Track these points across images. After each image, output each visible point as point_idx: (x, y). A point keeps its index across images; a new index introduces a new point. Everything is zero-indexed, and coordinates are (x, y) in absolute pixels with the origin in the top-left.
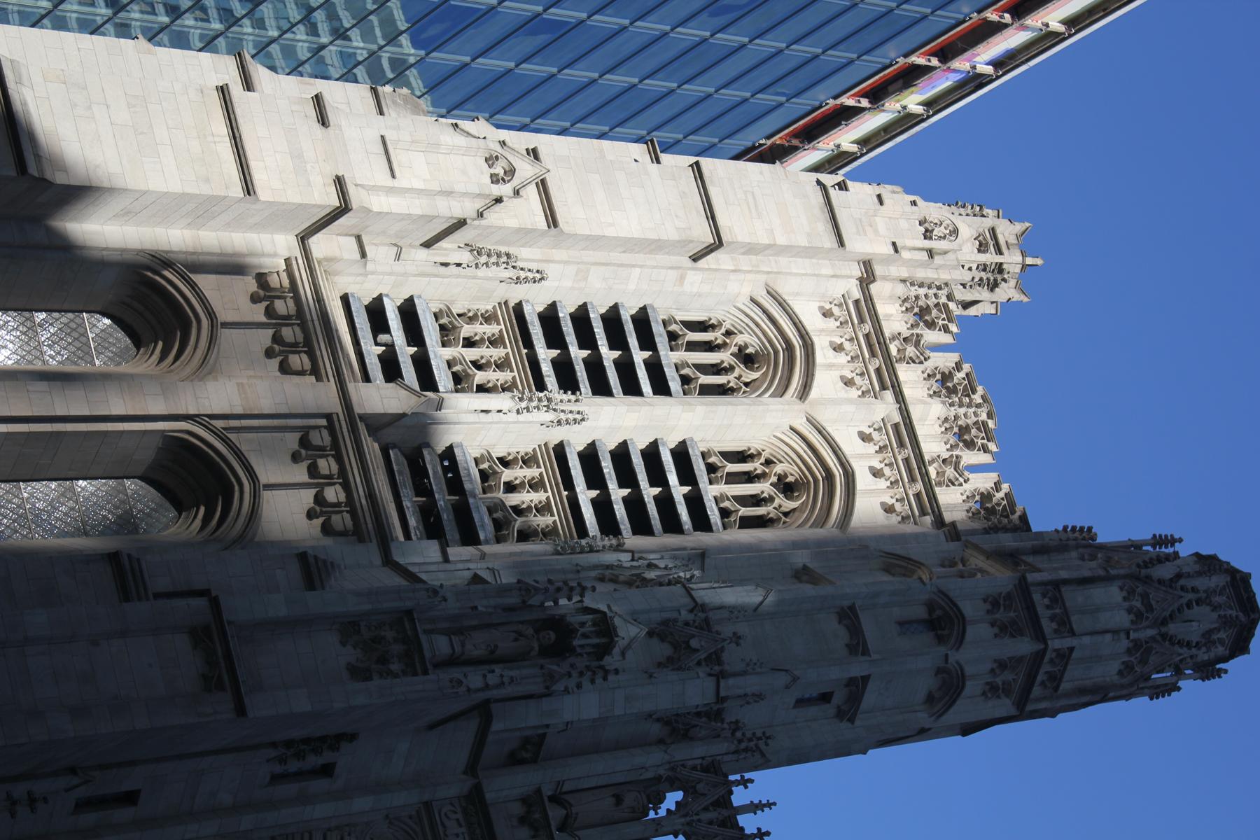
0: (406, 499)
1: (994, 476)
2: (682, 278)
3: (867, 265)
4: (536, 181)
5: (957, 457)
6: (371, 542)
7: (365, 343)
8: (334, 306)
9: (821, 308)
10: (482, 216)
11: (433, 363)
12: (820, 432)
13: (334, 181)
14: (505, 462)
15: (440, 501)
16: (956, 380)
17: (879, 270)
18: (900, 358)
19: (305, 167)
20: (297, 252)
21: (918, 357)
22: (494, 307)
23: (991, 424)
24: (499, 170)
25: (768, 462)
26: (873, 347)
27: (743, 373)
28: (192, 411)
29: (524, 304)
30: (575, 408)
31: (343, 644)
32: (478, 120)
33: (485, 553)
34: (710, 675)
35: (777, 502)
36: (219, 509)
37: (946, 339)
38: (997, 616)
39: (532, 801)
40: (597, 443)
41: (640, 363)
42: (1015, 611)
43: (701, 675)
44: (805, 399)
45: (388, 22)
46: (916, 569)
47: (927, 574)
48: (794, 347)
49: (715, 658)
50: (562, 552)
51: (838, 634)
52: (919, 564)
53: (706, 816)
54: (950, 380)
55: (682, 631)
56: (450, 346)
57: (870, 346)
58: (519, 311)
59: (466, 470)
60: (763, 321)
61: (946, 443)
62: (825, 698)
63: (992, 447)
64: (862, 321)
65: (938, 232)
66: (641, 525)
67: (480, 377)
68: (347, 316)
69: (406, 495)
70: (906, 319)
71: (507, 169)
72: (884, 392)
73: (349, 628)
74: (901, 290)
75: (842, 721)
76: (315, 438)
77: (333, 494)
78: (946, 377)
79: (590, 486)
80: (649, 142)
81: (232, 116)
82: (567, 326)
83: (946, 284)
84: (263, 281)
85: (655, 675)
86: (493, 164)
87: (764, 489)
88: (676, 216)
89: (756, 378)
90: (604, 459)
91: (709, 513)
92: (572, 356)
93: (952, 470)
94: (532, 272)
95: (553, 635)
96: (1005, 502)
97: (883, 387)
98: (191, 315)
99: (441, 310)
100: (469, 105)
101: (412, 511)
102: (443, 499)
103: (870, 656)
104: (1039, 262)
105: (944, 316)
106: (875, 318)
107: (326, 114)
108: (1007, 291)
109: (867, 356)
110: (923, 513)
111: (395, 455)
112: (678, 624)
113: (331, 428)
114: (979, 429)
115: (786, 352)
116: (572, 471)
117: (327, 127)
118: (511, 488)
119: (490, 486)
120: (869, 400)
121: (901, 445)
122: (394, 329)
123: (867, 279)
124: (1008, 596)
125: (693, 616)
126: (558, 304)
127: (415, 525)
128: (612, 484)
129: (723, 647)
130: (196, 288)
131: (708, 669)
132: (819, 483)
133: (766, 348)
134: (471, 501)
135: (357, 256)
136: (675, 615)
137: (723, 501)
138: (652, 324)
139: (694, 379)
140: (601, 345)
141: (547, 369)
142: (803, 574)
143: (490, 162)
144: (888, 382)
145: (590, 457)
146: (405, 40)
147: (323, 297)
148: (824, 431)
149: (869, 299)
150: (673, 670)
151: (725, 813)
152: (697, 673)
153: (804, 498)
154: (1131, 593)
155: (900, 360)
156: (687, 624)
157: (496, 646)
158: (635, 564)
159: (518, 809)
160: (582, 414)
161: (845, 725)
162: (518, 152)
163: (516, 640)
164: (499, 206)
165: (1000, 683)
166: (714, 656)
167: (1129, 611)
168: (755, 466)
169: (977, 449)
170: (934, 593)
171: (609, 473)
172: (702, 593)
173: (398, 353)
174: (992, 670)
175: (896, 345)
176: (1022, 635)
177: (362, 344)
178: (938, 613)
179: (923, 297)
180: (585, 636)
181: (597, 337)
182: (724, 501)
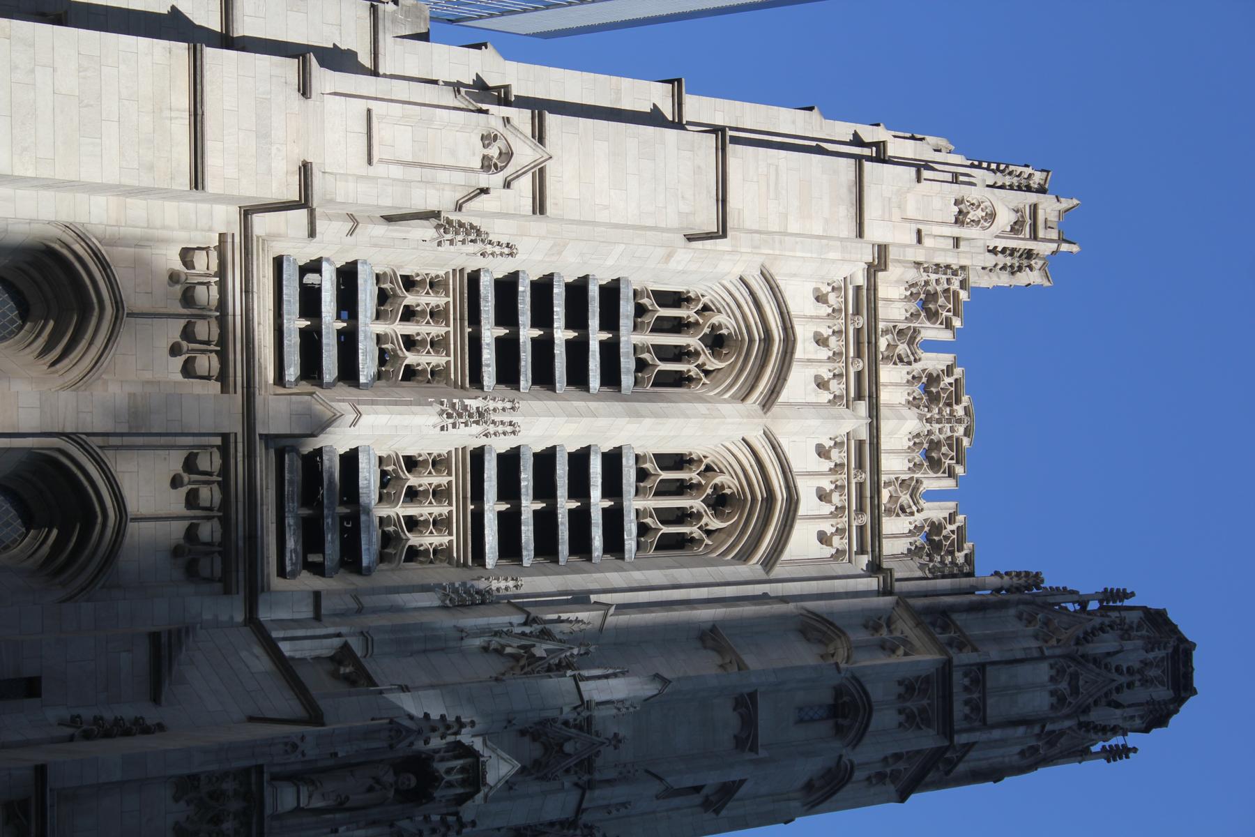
0: (290, 515)
1: (951, 505)
2: (669, 257)
3: (882, 249)
4: (533, 170)
5: (917, 481)
6: (238, 593)
7: (289, 319)
8: (264, 284)
9: (817, 290)
10: (460, 210)
11: (361, 346)
12: (774, 448)
13: (300, 168)
15: (327, 518)
16: (942, 385)
17: (893, 254)
18: (888, 357)
19: (270, 149)
20: (236, 229)
21: (908, 356)
22: (447, 273)
23: (966, 442)
24: (493, 152)
25: (706, 308)
26: (861, 345)
27: (707, 362)
28: (68, 430)
29: (482, 273)
30: (507, 419)
31: (176, 799)
32: (486, 48)
33: (363, 607)
34: (576, 785)
35: (705, 520)
36: (74, 539)
37: (946, 336)
38: (908, 704)
40: (522, 450)
41: (595, 351)
42: (929, 699)
43: (567, 785)
44: (768, 410)
46: (836, 637)
47: (846, 649)
48: (773, 340)
49: (587, 765)
50: (451, 605)
51: (729, 719)
52: (840, 632)
54: (935, 384)
55: (559, 733)
56: (385, 320)
57: (858, 343)
58: (474, 280)
59: (366, 480)
60: (747, 303)
61: (909, 461)
62: (697, 789)
63: (959, 470)
64: (857, 312)
66: (546, 547)
67: (410, 299)
68: (277, 341)
69: (292, 510)
70: (907, 307)
71: (504, 151)
72: (859, 402)
73: (186, 785)
74: (912, 275)
75: (705, 812)
76: (203, 463)
77: (208, 531)
78: (933, 379)
79: (499, 322)
80: (676, 83)
81: (199, 87)
82: (524, 303)
83: (963, 268)
84: (188, 259)
85: (516, 787)
86: (489, 145)
87: (693, 505)
88: (683, 197)
89: (720, 367)
90: (525, 469)
91: (626, 537)
92: (521, 341)
93: (908, 496)
94: (501, 246)
95: (413, 782)
96: (955, 536)
97: (859, 397)
98: (95, 300)
99: (385, 274)
101: (294, 529)
102: (334, 512)
103: (757, 753)
104: (1075, 249)
105: (951, 306)
106: (873, 312)
107: (310, 82)
108: (1032, 277)
109: (851, 354)
110: (861, 551)
111: (291, 460)
112: (556, 725)
113: (224, 450)
115: (762, 344)
116: (485, 484)
117: (307, 98)
118: (413, 495)
119: (389, 494)
121: (860, 466)
122: (325, 302)
124: (927, 680)
125: (576, 714)
126: (521, 274)
127: (293, 547)
128: (527, 500)
129: (599, 751)
130: (108, 270)
131: (575, 779)
132: (757, 503)
133: (741, 333)
134: (363, 518)
135: (305, 232)
136: (555, 714)
137: (643, 352)
138: (621, 302)
139: (652, 365)
140: (557, 328)
141: (489, 356)
143: (486, 142)
145: (509, 462)
147: (254, 384)
148: (779, 449)
149: (873, 288)
150: (537, 778)
152: (563, 784)
153: (736, 518)
154: (1061, 672)
155: (887, 359)
156: (566, 723)
157: (347, 798)
158: (527, 630)
160: (514, 425)
161: (710, 815)
162: (521, 133)
163: (370, 789)
164: (484, 196)
165: (889, 773)
166: (586, 763)
167: (1052, 693)
169: (942, 470)
170: (847, 678)
171: (527, 486)
172: (592, 684)
173: (324, 333)
174: (885, 759)
175: (887, 339)
176: (929, 725)
177: (285, 321)
178: (846, 699)
179: (934, 281)
180: (450, 785)
181: (555, 317)
182: (647, 518)
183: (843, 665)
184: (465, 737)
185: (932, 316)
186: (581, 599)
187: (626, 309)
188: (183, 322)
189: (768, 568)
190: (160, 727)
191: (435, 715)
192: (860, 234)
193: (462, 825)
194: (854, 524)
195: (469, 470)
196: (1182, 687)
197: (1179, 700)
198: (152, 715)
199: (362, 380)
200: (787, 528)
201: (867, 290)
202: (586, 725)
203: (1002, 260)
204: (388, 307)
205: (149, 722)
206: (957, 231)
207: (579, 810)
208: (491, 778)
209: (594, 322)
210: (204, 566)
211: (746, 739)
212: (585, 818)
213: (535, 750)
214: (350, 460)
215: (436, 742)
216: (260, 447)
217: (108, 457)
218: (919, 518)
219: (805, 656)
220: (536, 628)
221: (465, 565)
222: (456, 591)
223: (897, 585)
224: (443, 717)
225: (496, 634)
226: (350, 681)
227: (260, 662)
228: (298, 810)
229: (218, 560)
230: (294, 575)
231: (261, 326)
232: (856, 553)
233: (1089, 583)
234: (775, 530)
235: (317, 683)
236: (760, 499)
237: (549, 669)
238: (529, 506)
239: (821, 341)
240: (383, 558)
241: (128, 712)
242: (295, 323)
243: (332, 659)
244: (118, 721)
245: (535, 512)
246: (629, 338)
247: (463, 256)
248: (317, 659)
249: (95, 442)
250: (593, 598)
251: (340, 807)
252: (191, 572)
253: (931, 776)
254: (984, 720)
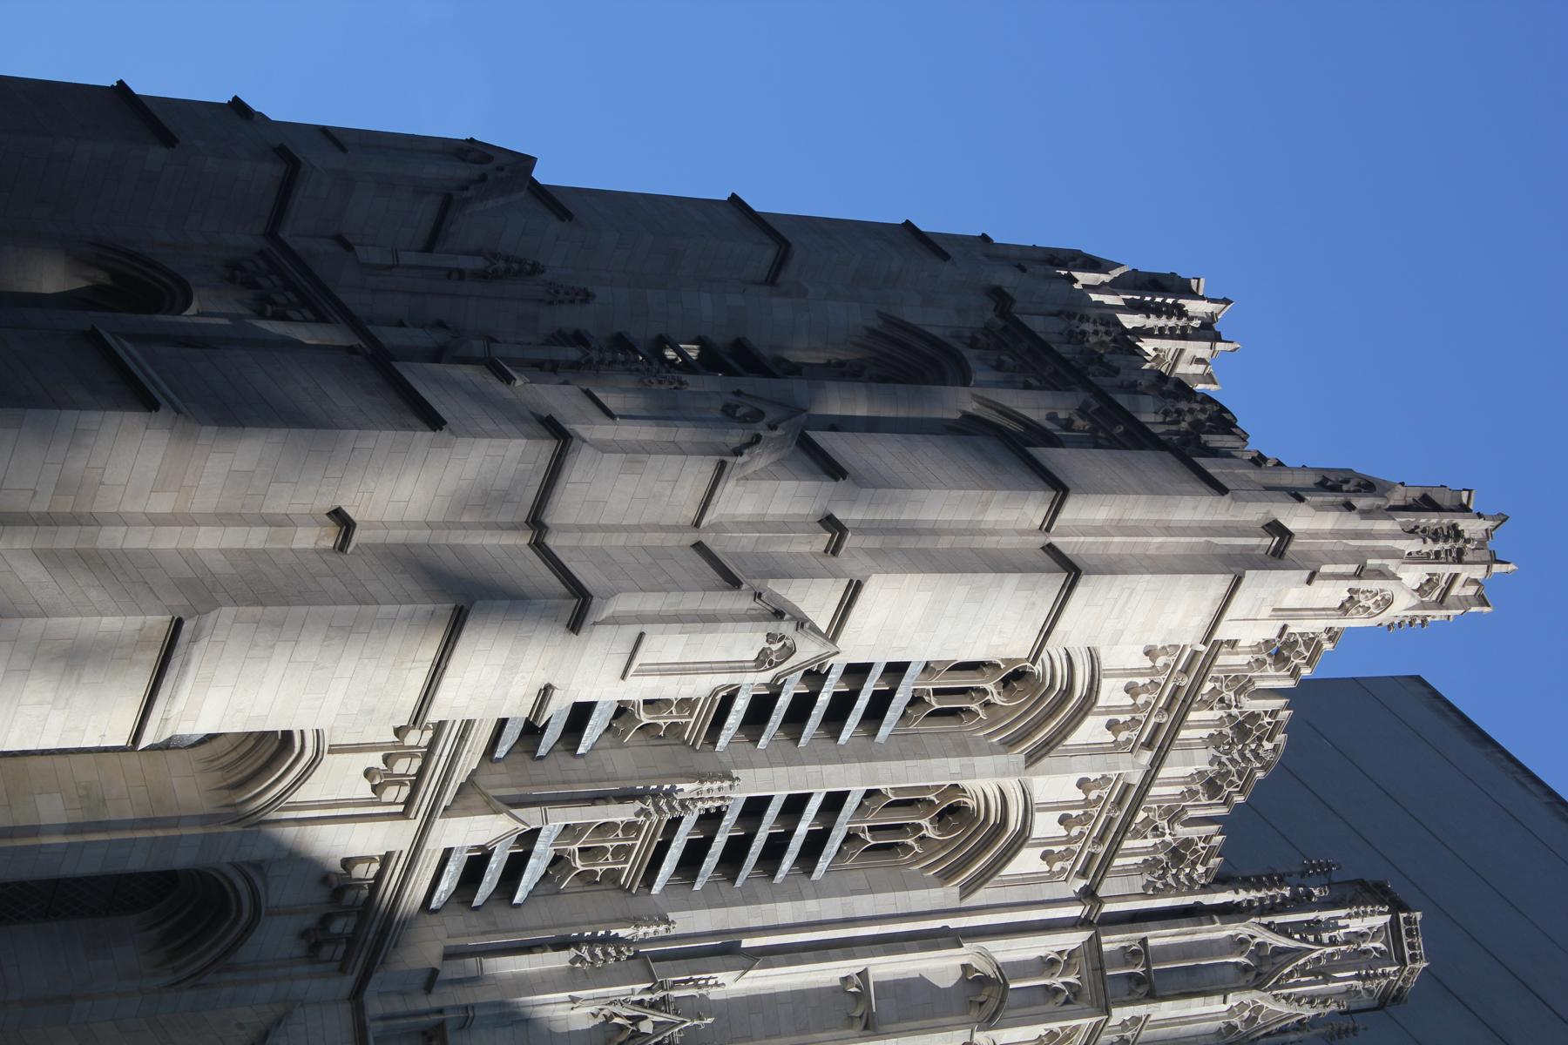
13: (540, 690)
18: (1206, 701)
21: (1230, 700)
26: (1175, 700)
47: (998, 1001)
57: (1173, 697)
97: (1148, 745)
106: (1202, 677)
110: (1083, 874)
115: (1060, 695)
133: (1044, 677)
149: (1212, 656)
189: (1032, 760)
195: (714, 711)
200: (1005, 859)
201: (1159, 748)
231: (470, 754)
232: (1142, 744)
234: (1057, 724)
236: (1058, 689)
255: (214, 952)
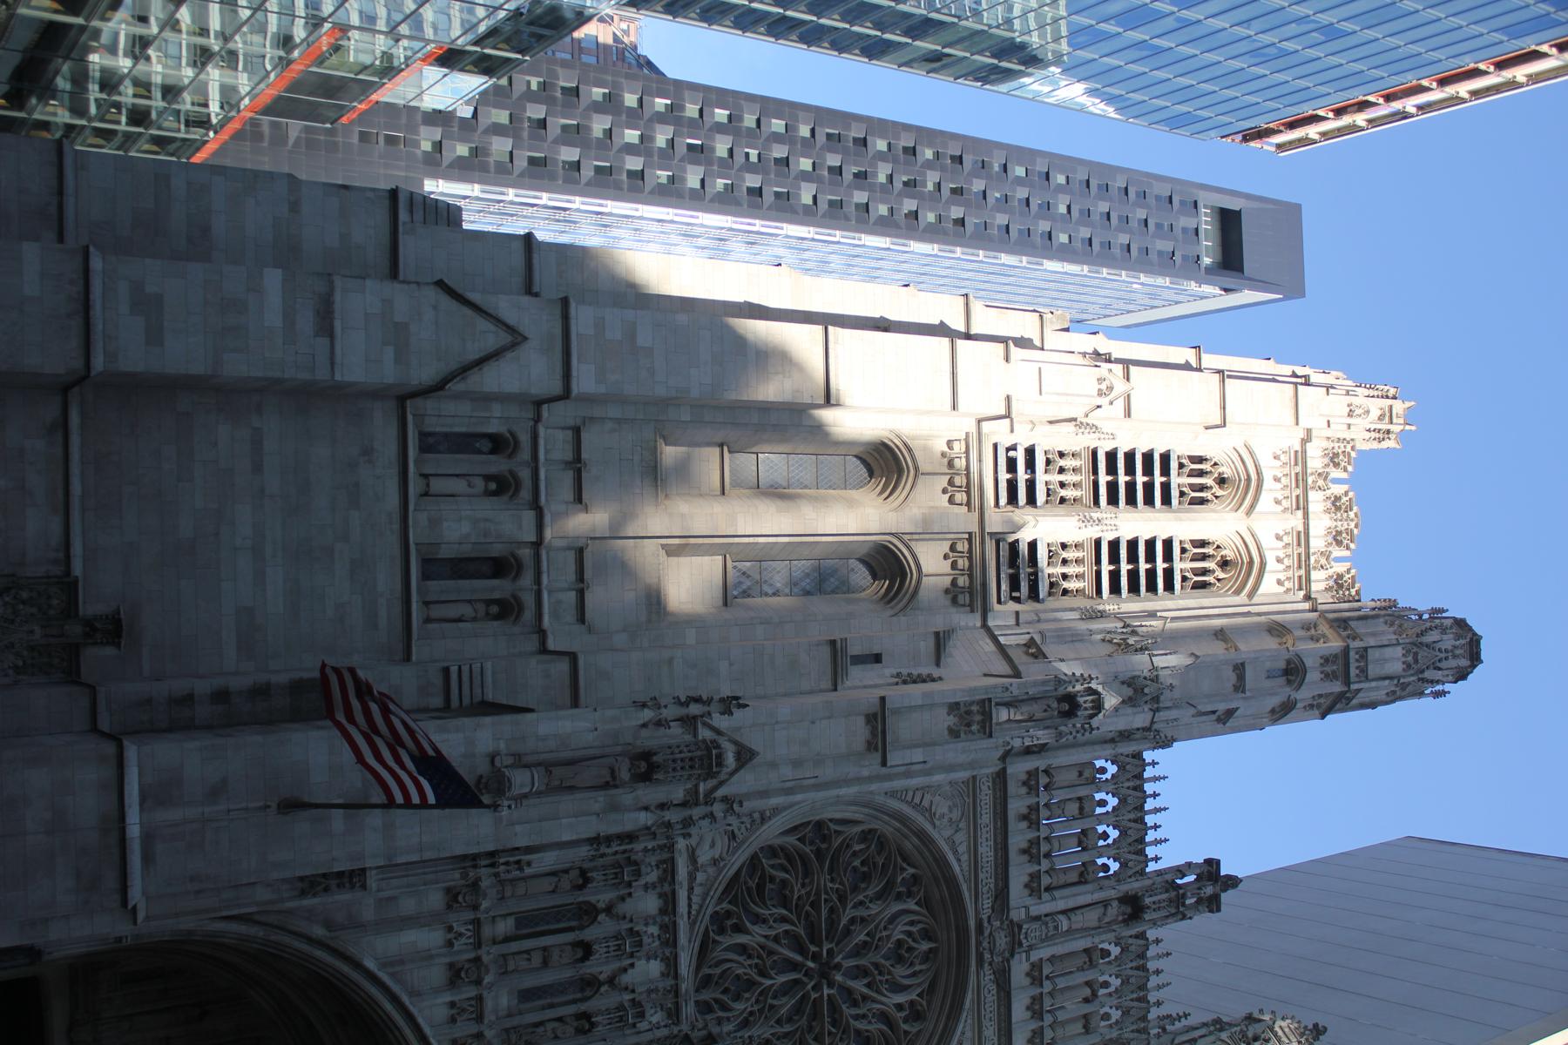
3: (1309, 431)
14: (1061, 455)
17: (1314, 433)
23: (1356, 531)
24: (1103, 387)
30: (1113, 523)
31: (949, 714)
35: (1217, 573)
37: (1344, 475)
39: (1033, 774)
45: (1057, 31)
49: (1156, 699)
51: (1232, 678)
52: (1289, 631)
53: (1127, 784)
57: (1297, 480)
58: (1094, 453)
62: (1214, 712)
63: (1352, 546)
64: (1296, 464)
65: (1358, 411)
66: (1134, 588)
67: (1062, 463)
73: (954, 707)
74: (1326, 444)
76: (959, 547)
77: (962, 581)
78: (1337, 499)
83: (1352, 440)
95: (1067, 708)
97: (1298, 508)
100: (1093, 79)
104: (1413, 428)
108: (1390, 444)
109: (1293, 486)
113: (970, 540)
114: (1347, 534)
118: (1065, 562)
120: (1288, 515)
121: (1299, 545)
123: (1306, 440)
124: (1336, 656)
142: (1220, 634)
144: (1302, 505)
145: (1114, 545)
146: (1064, 42)
151: (1138, 782)
154: (1409, 651)
156: (1145, 678)
158: (1125, 630)
159: (1024, 777)
163: (1045, 711)
167: (1404, 663)
168: (1208, 550)
174: (1313, 697)
180: (1086, 709)
183: (1291, 649)
184: (1094, 685)
185: (1336, 465)
186: (1152, 615)
187: (1174, 465)
188: (949, 477)
190: (940, 679)
191: (1078, 674)
192: (1297, 424)
193: (1092, 729)
194: (1296, 575)
196: (1475, 658)
197: (1474, 667)
198: (936, 673)
199: (1038, 504)
202: (1156, 679)
203: (1373, 435)
204: (1050, 467)
205: (935, 675)
206: (1350, 421)
207: (1152, 722)
208: (1107, 706)
209: (1157, 471)
210: (961, 599)
211: (1240, 686)
212: (1155, 726)
213: (1129, 692)
214: (1033, 546)
215: (1079, 687)
216: (987, 538)
217: (912, 544)
218: (1331, 572)
219: (1271, 643)
220: (1129, 629)
221: (1092, 597)
222: (1088, 611)
223: (1320, 607)
224: (1082, 675)
225: (1109, 632)
226: (1035, 656)
227: (990, 647)
228: (1009, 720)
229: (967, 595)
230: (1005, 603)
233: (1423, 605)
235: (1019, 657)
237: (1136, 651)
238: (1125, 567)
239: (1277, 480)
240: (1050, 594)
241: (924, 671)
242: (1004, 476)
243: (1025, 645)
244: (919, 676)
245: (1128, 570)
246: (1175, 480)
247: (1089, 441)
248: (1018, 645)
249: (906, 537)
250: (1159, 614)
251: (1030, 719)
252: (954, 601)
253: (1338, 706)
254: (1367, 677)
255: (905, 601)
